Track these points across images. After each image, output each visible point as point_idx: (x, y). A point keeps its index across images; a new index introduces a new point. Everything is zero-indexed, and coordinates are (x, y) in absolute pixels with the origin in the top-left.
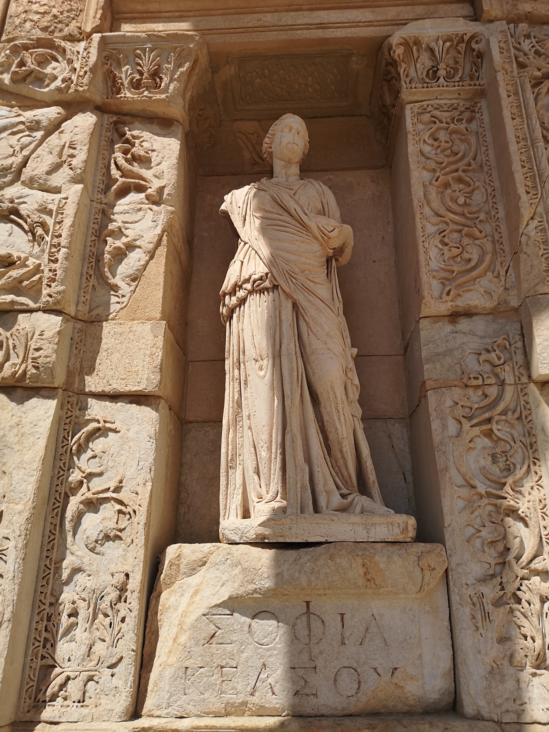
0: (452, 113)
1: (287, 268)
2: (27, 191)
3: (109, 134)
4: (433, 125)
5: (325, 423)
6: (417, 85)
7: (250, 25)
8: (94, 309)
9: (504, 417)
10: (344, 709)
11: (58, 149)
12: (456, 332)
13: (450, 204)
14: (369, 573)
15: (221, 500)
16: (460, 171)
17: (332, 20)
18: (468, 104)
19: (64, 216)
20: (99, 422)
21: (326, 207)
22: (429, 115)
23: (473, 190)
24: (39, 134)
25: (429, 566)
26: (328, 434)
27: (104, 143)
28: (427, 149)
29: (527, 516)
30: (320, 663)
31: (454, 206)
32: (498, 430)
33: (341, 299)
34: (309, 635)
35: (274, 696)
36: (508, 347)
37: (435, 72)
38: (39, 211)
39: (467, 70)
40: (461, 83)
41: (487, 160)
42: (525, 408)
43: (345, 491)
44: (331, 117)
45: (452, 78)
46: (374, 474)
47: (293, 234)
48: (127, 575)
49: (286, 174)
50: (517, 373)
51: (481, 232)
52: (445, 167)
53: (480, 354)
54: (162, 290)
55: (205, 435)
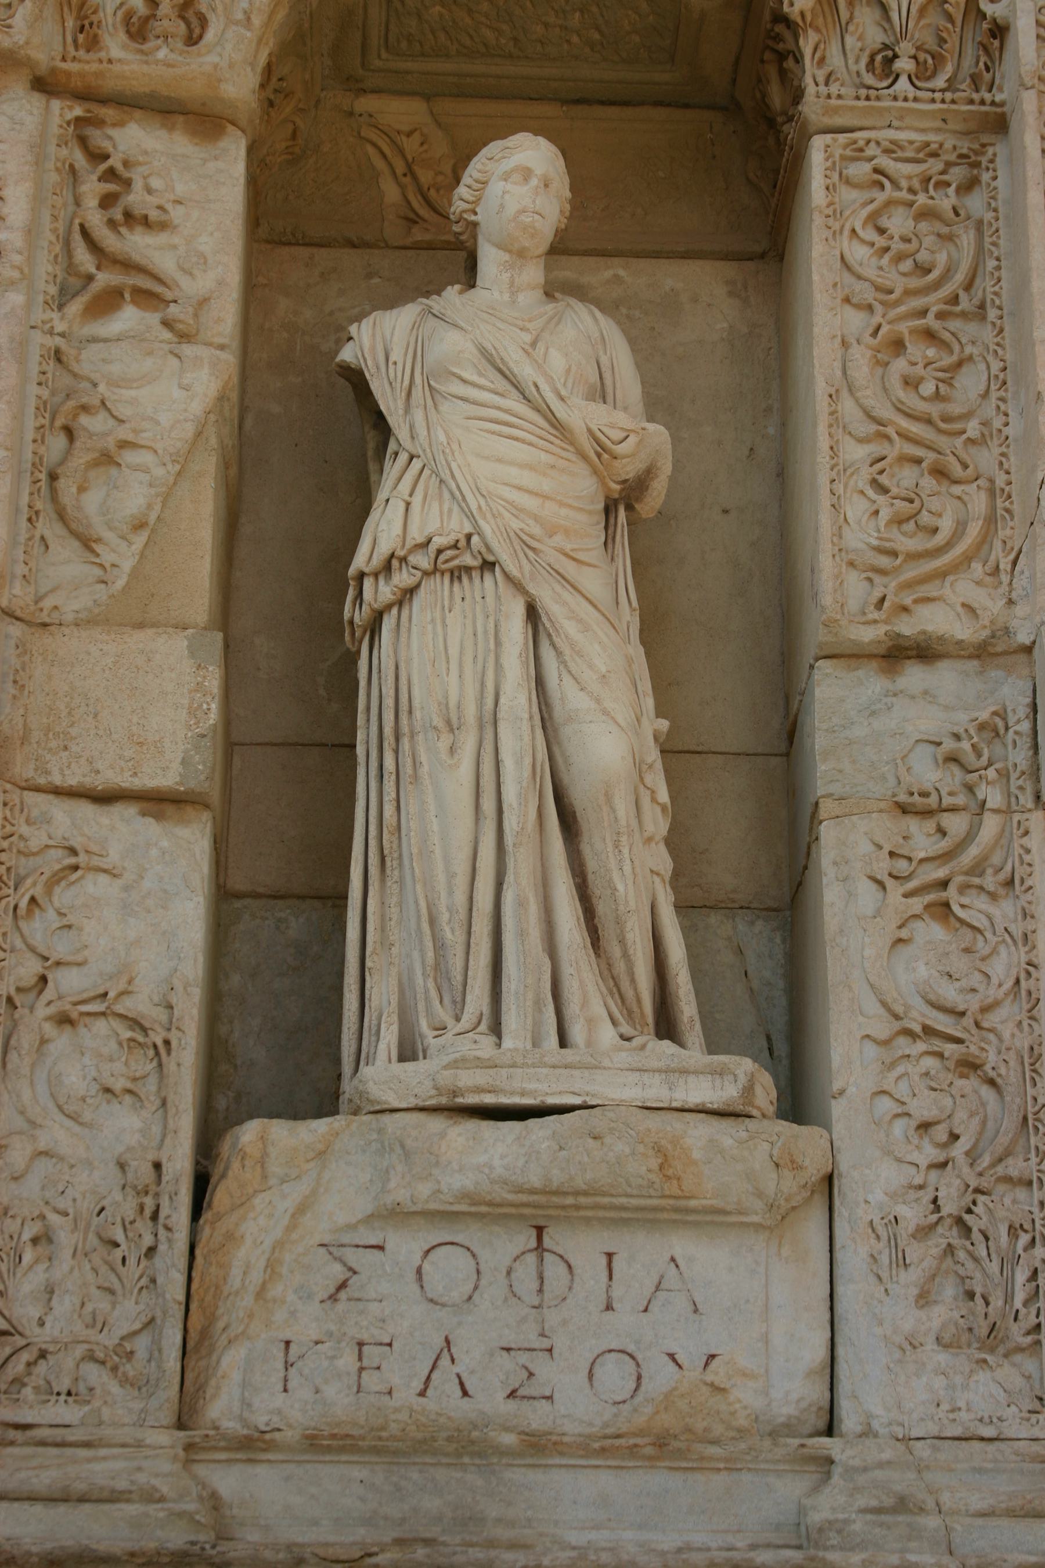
0: (922, 167)
1: (516, 525)
3: (64, 152)
4: (876, 193)
5: (590, 877)
6: (843, 91)
8: (46, 595)
9: (977, 881)
10: (606, 1425)
12: (895, 695)
13: (901, 394)
14: (670, 1166)
16: (931, 316)
20: (73, 852)
22: (867, 167)
23: (960, 364)
25: (793, 1162)
26: (594, 901)
27: (54, 177)
28: (859, 253)
29: (999, 1075)
30: (560, 1343)
32: (963, 906)
34: (540, 1291)
35: (466, 1399)
36: (1002, 731)
37: (889, 61)
39: (968, 62)
40: (948, 96)
41: (996, 294)
42: (1022, 862)
43: (626, 1029)
44: (626, 104)
46: (694, 1004)
47: (530, 444)
48: (157, 1166)
49: (512, 284)
50: (1013, 789)
51: (965, 466)
52: (897, 303)
53: (939, 744)
54: (208, 559)
55: (278, 928)
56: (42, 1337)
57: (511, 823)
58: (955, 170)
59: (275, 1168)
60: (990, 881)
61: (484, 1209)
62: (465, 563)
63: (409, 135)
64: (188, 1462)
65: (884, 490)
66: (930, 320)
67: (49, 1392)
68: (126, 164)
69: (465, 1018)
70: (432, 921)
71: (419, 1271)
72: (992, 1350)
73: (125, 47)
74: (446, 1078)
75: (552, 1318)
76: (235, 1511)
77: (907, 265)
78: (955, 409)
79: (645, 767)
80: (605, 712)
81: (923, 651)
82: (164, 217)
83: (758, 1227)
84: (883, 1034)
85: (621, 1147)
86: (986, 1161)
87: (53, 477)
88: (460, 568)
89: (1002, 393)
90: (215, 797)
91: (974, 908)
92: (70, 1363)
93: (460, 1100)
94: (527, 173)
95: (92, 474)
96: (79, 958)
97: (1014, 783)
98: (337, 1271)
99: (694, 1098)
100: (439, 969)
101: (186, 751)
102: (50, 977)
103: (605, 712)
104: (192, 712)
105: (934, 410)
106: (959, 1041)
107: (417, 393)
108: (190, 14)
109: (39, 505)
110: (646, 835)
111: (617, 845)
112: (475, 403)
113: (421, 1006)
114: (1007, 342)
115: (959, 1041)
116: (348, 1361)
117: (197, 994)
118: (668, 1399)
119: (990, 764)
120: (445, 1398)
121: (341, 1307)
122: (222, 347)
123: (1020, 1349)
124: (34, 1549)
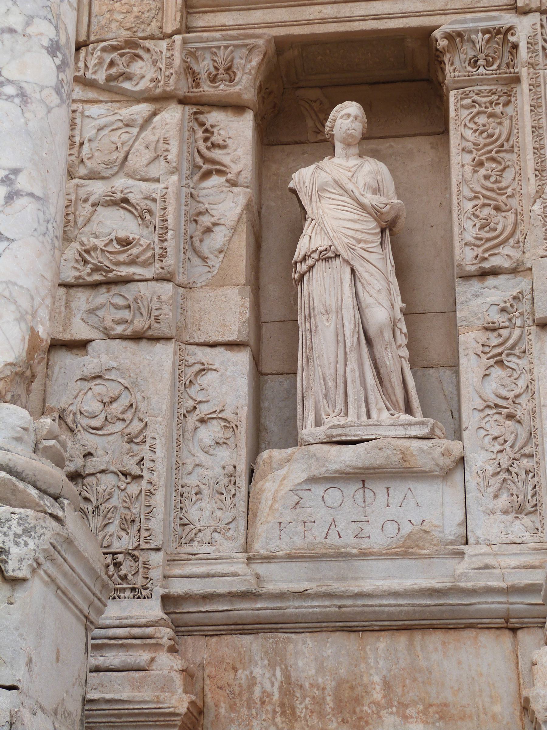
0: (490, 98)
1: (346, 241)
2: (131, 182)
3: (191, 124)
7: (312, 17)
10: (388, 545)
11: (154, 145)
13: (483, 181)
15: (298, 422)
16: (493, 152)
17: (386, 11)
18: (505, 89)
19: (166, 203)
21: (380, 184)
22: (469, 101)
23: (505, 169)
24: (135, 131)
30: (372, 519)
31: (488, 184)
33: (393, 264)
37: (476, 62)
38: (144, 198)
40: (498, 71)
43: (393, 411)
45: (491, 66)
48: (235, 467)
49: (346, 155)
51: (506, 205)
52: (481, 149)
54: (244, 261)
57: (348, 344)
58: (502, 98)
59: (274, 466)
60: (517, 351)
61: (344, 475)
62: (328, 256)
63: (315, 102)
64: (248, 564)
65: (478, 217)
66: (493, 154)
67: (201, 542)
68: (212, 126)
69: (336, 411)
70: (324, 379)
71: (323, 497)
72: (521, 513)
73: (209, 86)
74: (329, 432)
75: (369, 510)
76: (265, 579)
77: (485, 134)
78: (503, 185)
79: (397, 321)
80: (379, 303)
81: (494, 272)
82: (225, 143)
83: (437, 477)
84: (481, 408)
85: (389, 452)
86: (517, 448)
87: (191, 237)
88: (328, 258)
89: (520, 178)
90: (252, 342)
91: (512, 362)
92: (209, 533)
93: (334, 439)
94: (349, 115)
95: (204, 236)
96: (206, 399)
97: (526, 316)
98: (296, 499)
100: (326, 396)
101: (239, 327)
102: (197, 406)
103: (379, 303)
104: (240, 314)
105: (495, 186)
106: (507, 408)
107: (314, 197)
108: (230, 72)
109: (187, 247)
110: (398, 344)
111: (386, 349)
112: (333, 199)
113: (322, 408)
114: (521, 160)
115: (507, 408)
116: (300, 528)
117: (246, 409)
118: (409, 536)
119: (517, 310)
120: (333, 539)
121: (298, 510)
122: (247, 187)
123: (530, 513)
124: (198, 593)
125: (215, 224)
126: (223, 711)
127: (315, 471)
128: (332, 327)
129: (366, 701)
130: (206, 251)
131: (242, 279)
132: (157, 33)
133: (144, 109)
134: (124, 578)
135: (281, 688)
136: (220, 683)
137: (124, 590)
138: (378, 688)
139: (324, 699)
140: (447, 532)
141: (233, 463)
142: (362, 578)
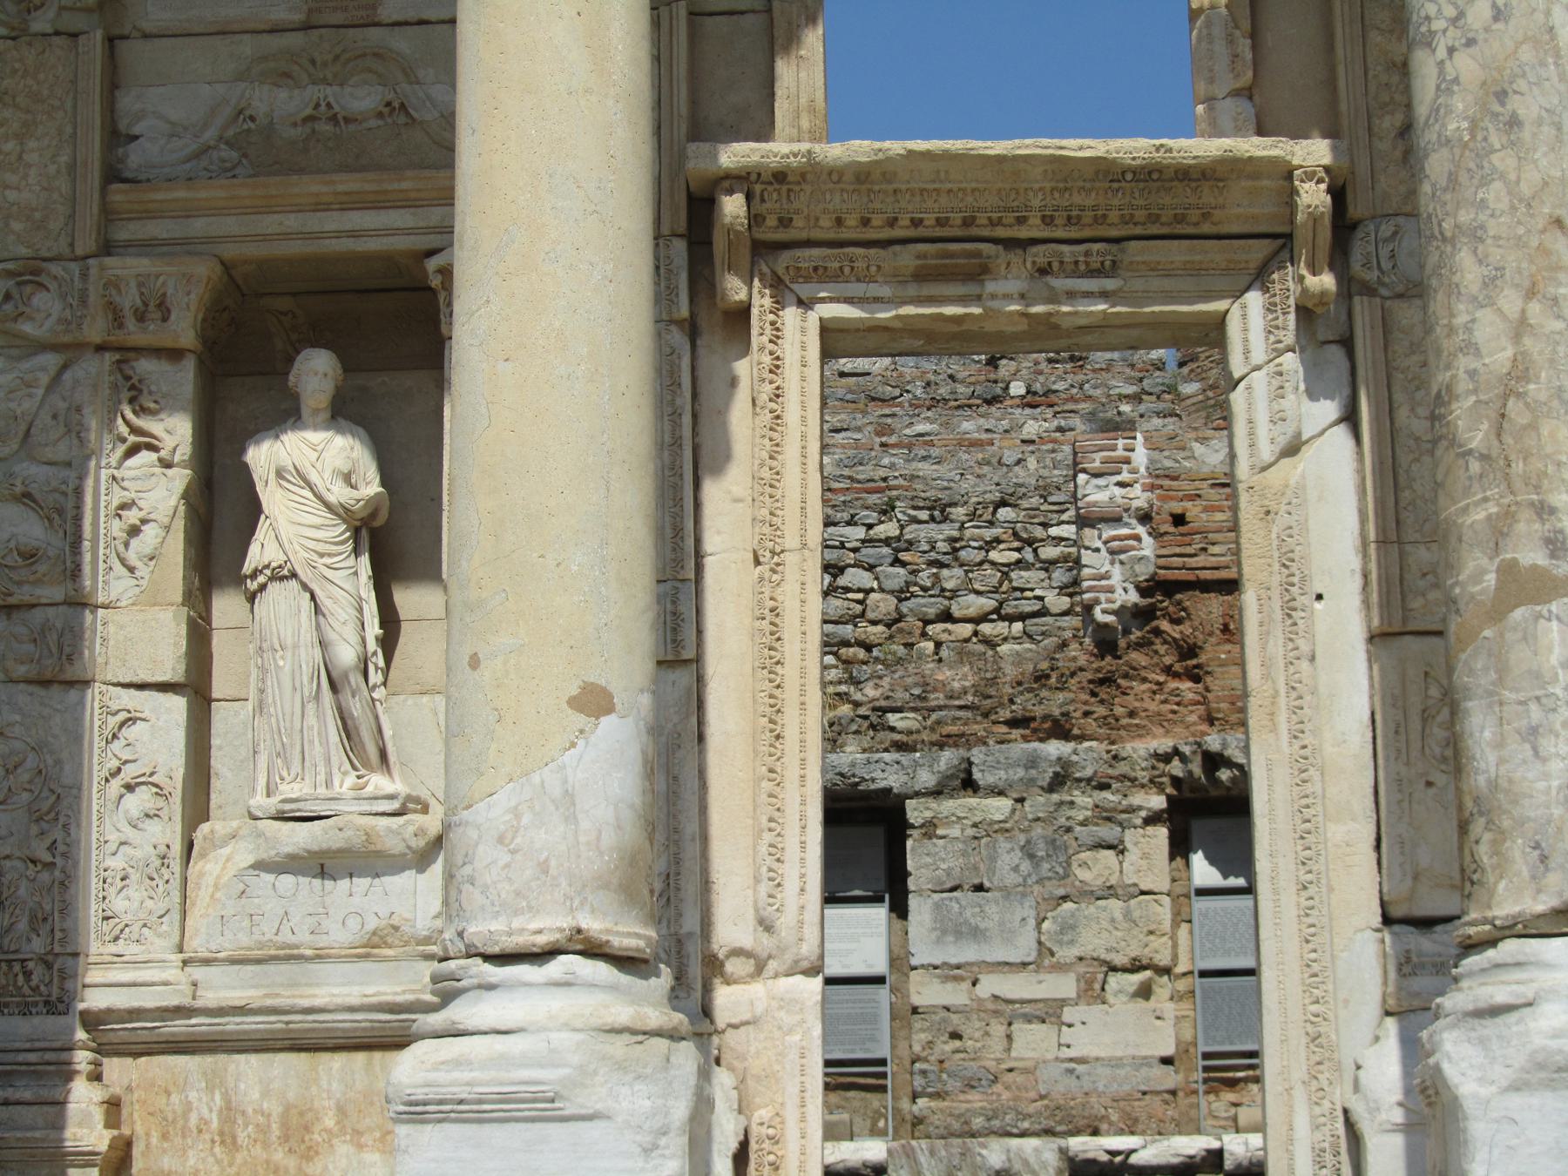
7: (269, 231)
17: (366, 226)
56: (126, 919)
63: (285, 314)
75: (328, 900)
98: (241, 887)
99: (381, 809)
116: (246, 923)
118: (374, 933)
121: (243, 900)
125: (144, 521)
126: (154, 1141)
127: (265, 854)
128: (287, 669)
129: (317, 1128)
130: (132, 558)
131: (178, 597)
132: (67, 251)
133: (51, 360)
134: (35, 989)
135: (221, 1111)
136: (151, 1109)
137: (36, 1004)
138: (331, 1113)
139: (269, 1126)
140: (419, 925)
141: (166, 841)
142: (318, 985)
